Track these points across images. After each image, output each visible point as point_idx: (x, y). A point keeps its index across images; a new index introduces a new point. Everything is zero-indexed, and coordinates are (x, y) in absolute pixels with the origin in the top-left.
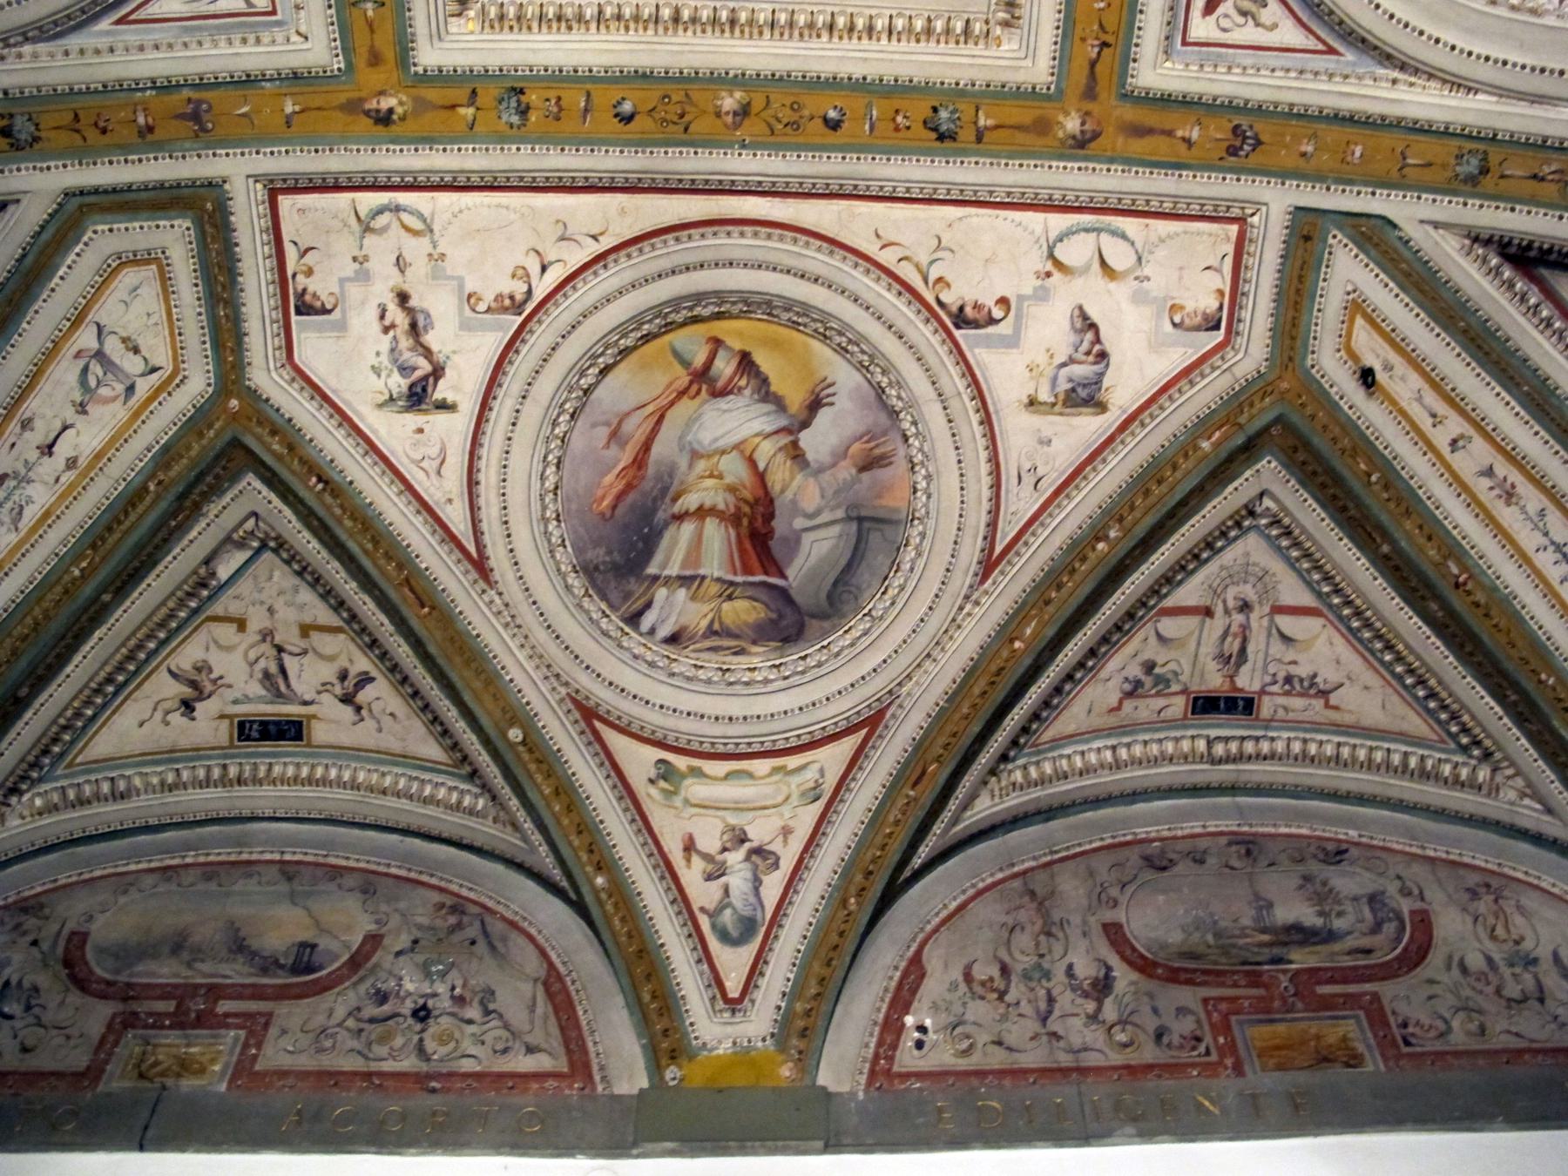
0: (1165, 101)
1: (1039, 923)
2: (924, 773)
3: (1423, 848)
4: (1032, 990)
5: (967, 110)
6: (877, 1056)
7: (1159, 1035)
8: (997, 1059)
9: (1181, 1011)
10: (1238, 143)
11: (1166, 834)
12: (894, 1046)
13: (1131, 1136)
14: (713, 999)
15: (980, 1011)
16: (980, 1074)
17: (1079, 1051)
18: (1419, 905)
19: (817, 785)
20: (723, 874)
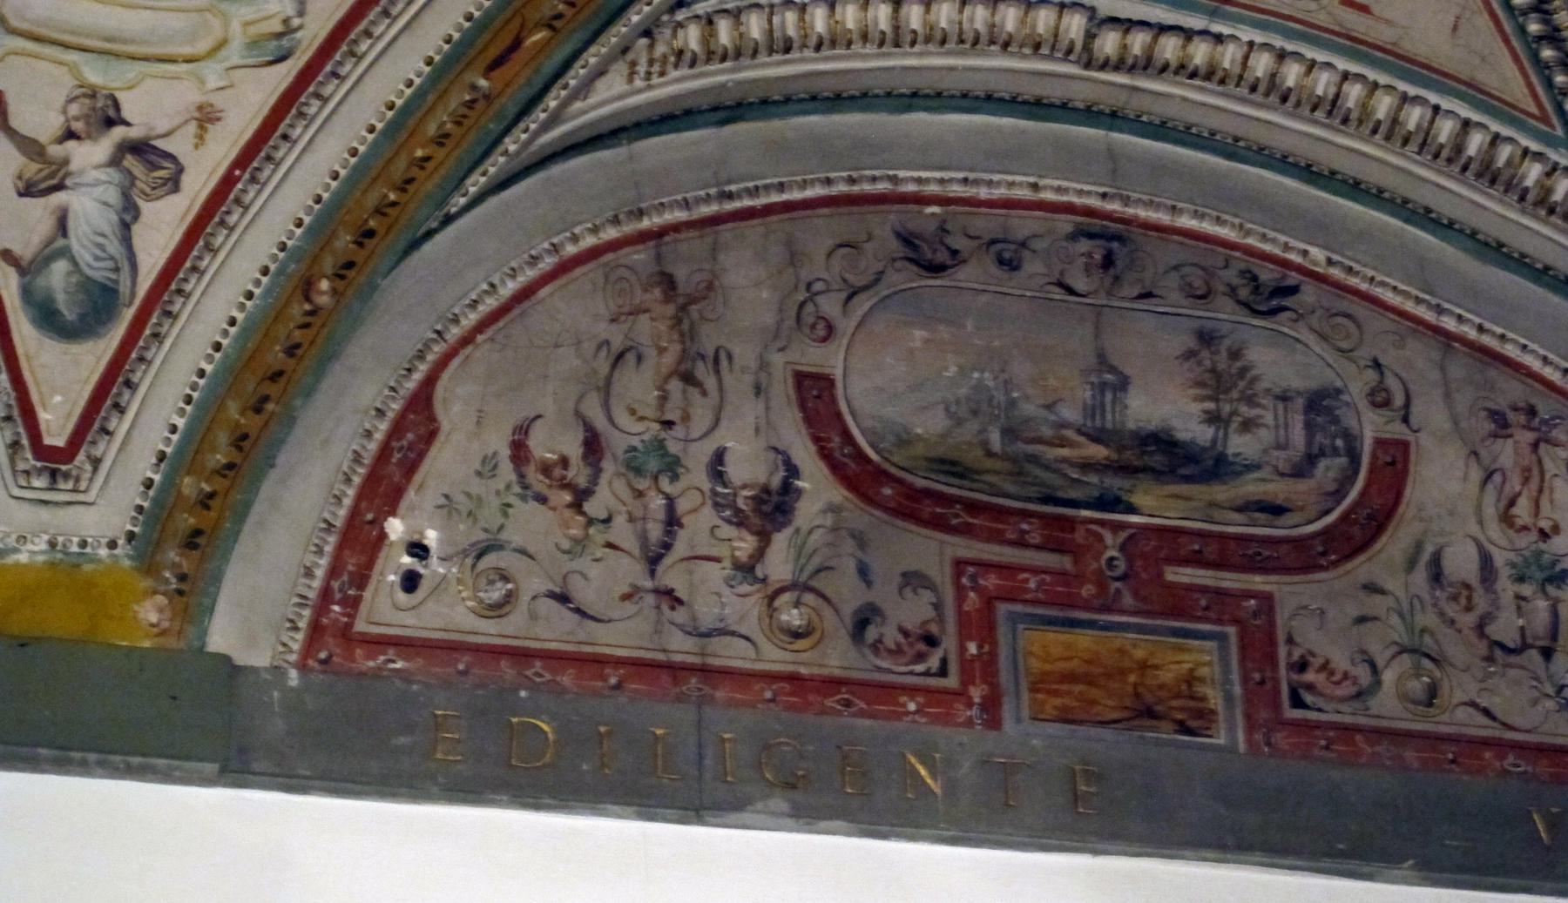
1: (675, 349)
2: (516, 44)
3: (1440, 310)
4: (640, 494)
6: (326, 594)
7: (861, 623)
8: (555, 630)
9: (913, 580)
11: (957, 190)
12: (361, 579)
13: (773, 813)
14: (15, 446)
15: (536, 525)
16: (521, 656)
17: (707, 635)
18: (1397, 430)
19: (288, 30)
20: (60, 187)
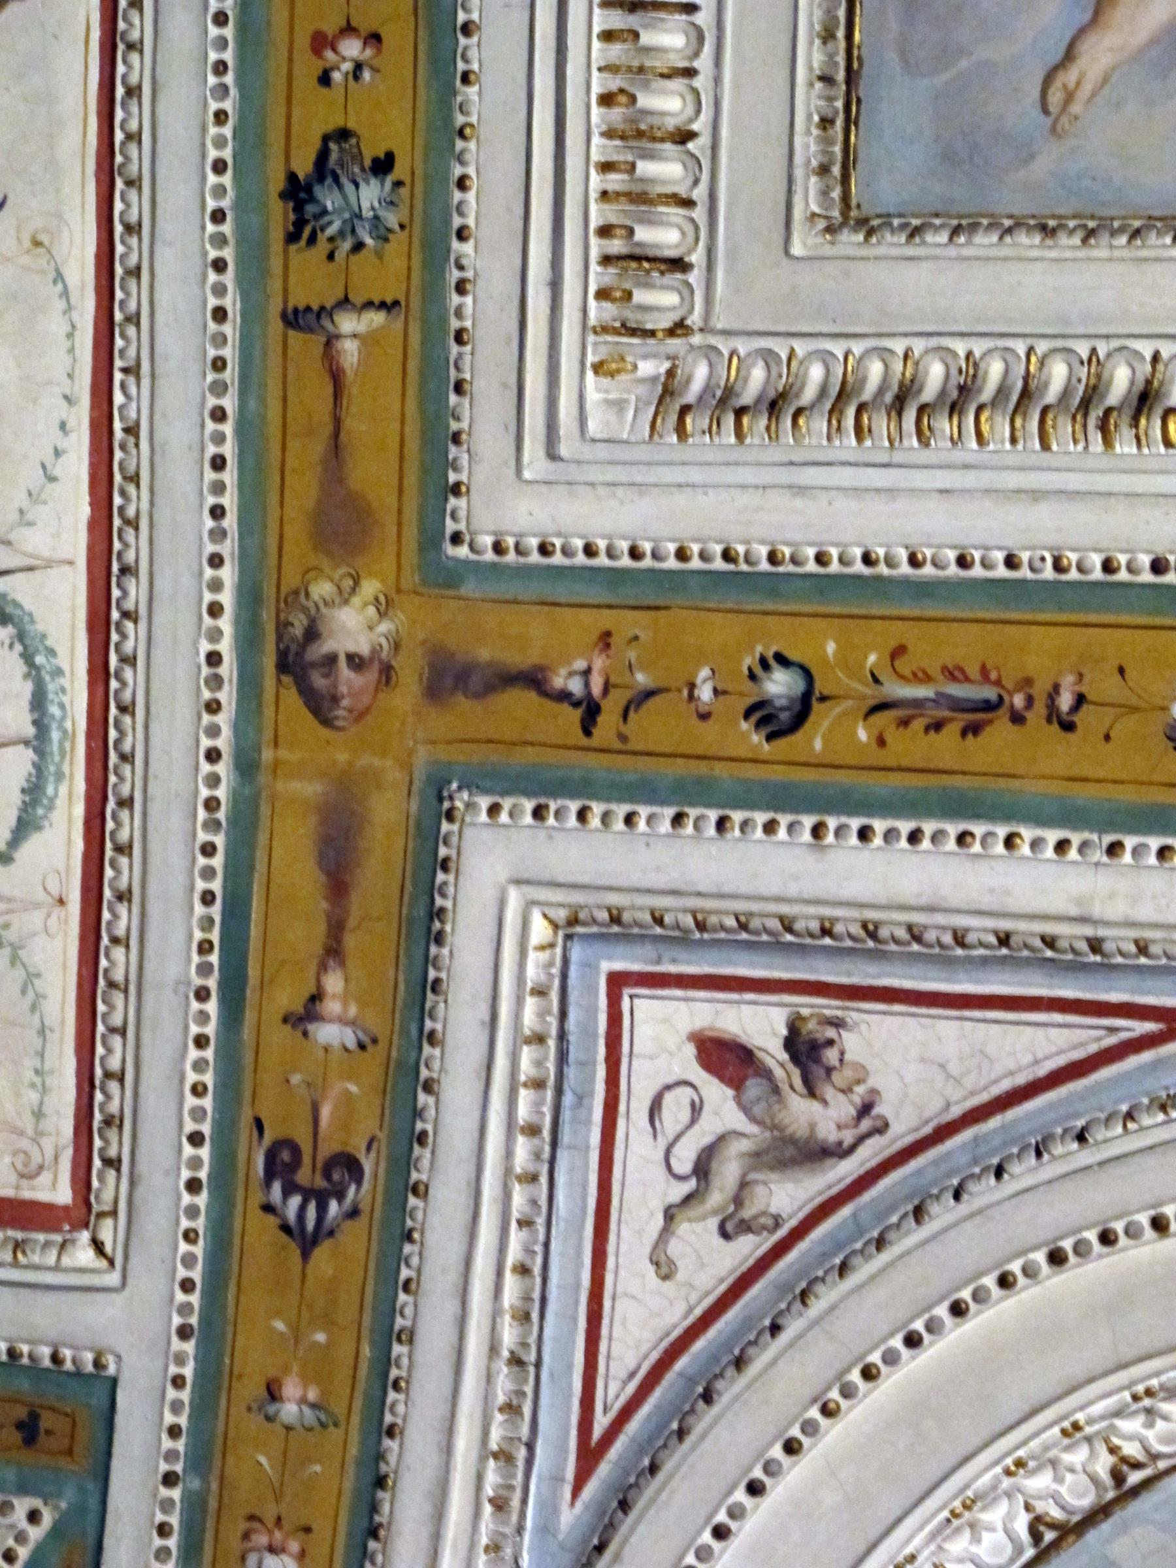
0: (426, 925)
5: (382, 273)
10: (303, 1176)
